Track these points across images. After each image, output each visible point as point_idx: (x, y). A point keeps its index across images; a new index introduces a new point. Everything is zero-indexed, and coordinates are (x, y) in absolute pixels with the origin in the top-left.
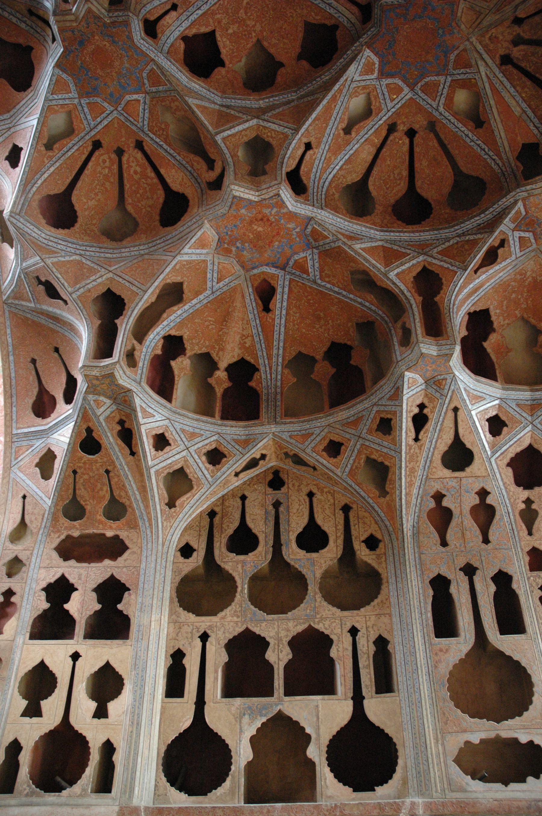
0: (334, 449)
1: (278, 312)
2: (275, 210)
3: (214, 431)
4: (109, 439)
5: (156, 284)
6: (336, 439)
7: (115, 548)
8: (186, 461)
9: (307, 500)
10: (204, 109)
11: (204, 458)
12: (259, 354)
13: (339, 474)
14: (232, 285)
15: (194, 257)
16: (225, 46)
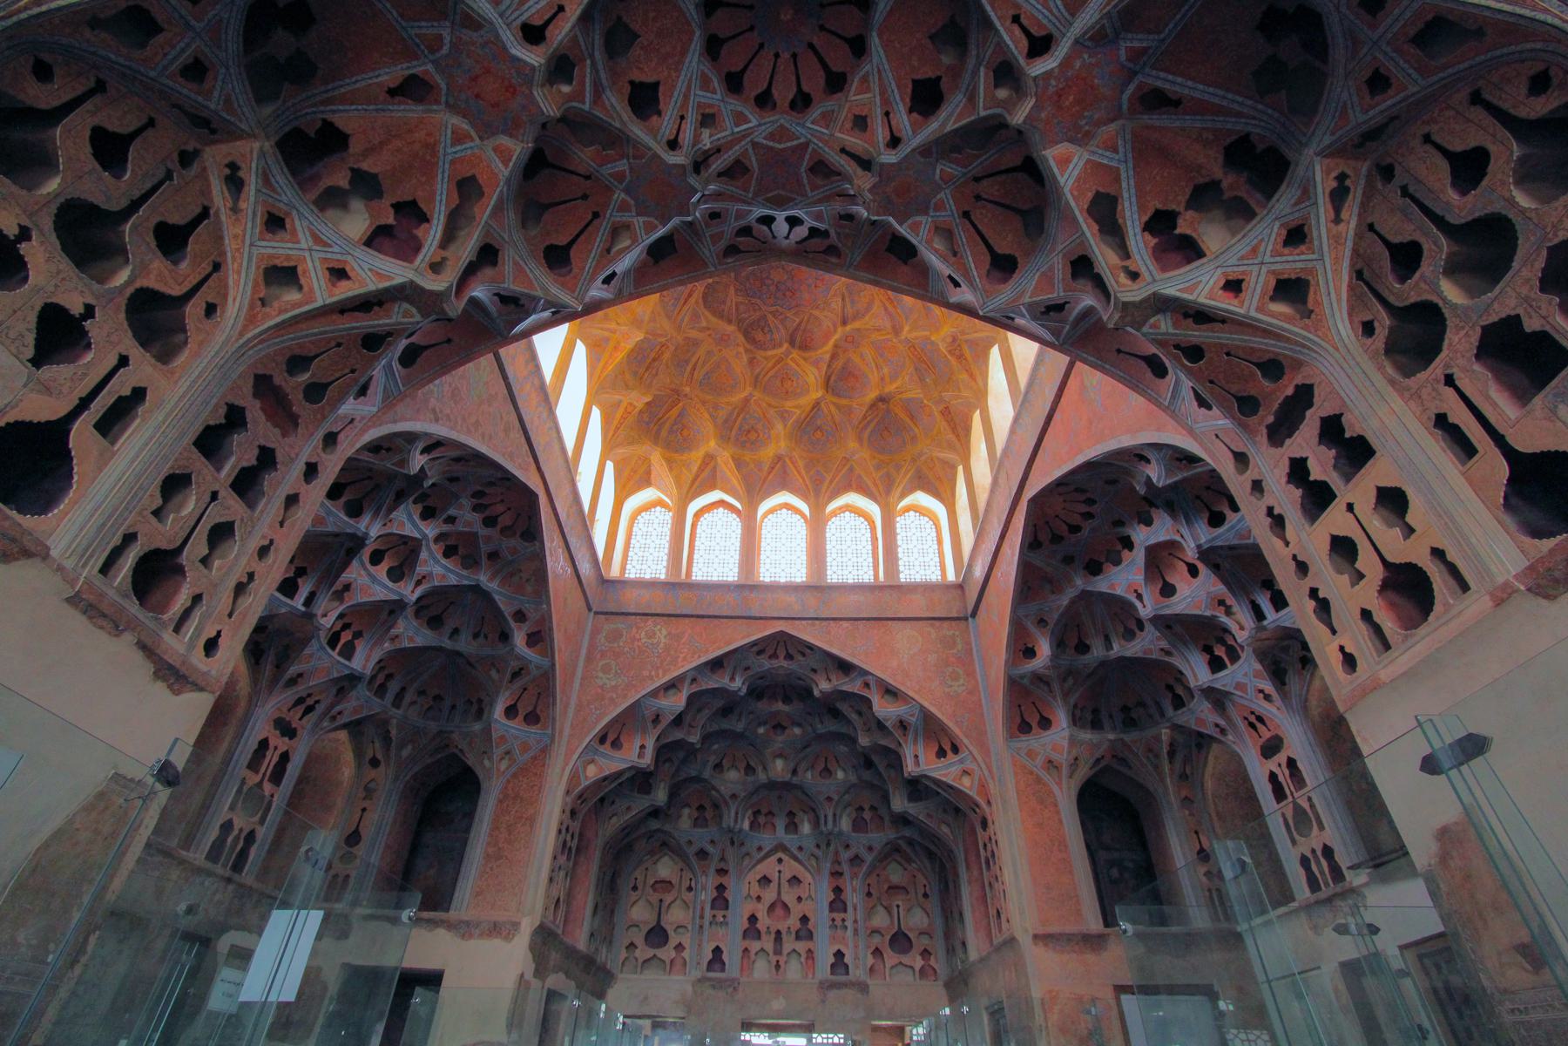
0: (1378, 82)
1: (1186, 91)
2: (1053, 82)
3: (1267, 229)
4: (1196, 334)
5: (1081, 220)
6: (1367, 74)
7: (1304, 396)
8: (1274, 272)
9: (1428, 147)
10: (958, 119)
11: (1286, 251)
12: (1229, 126)
13: (1415, 89)
14: (1128, 137)
15: (1076, 173)
16: (927, 73)
